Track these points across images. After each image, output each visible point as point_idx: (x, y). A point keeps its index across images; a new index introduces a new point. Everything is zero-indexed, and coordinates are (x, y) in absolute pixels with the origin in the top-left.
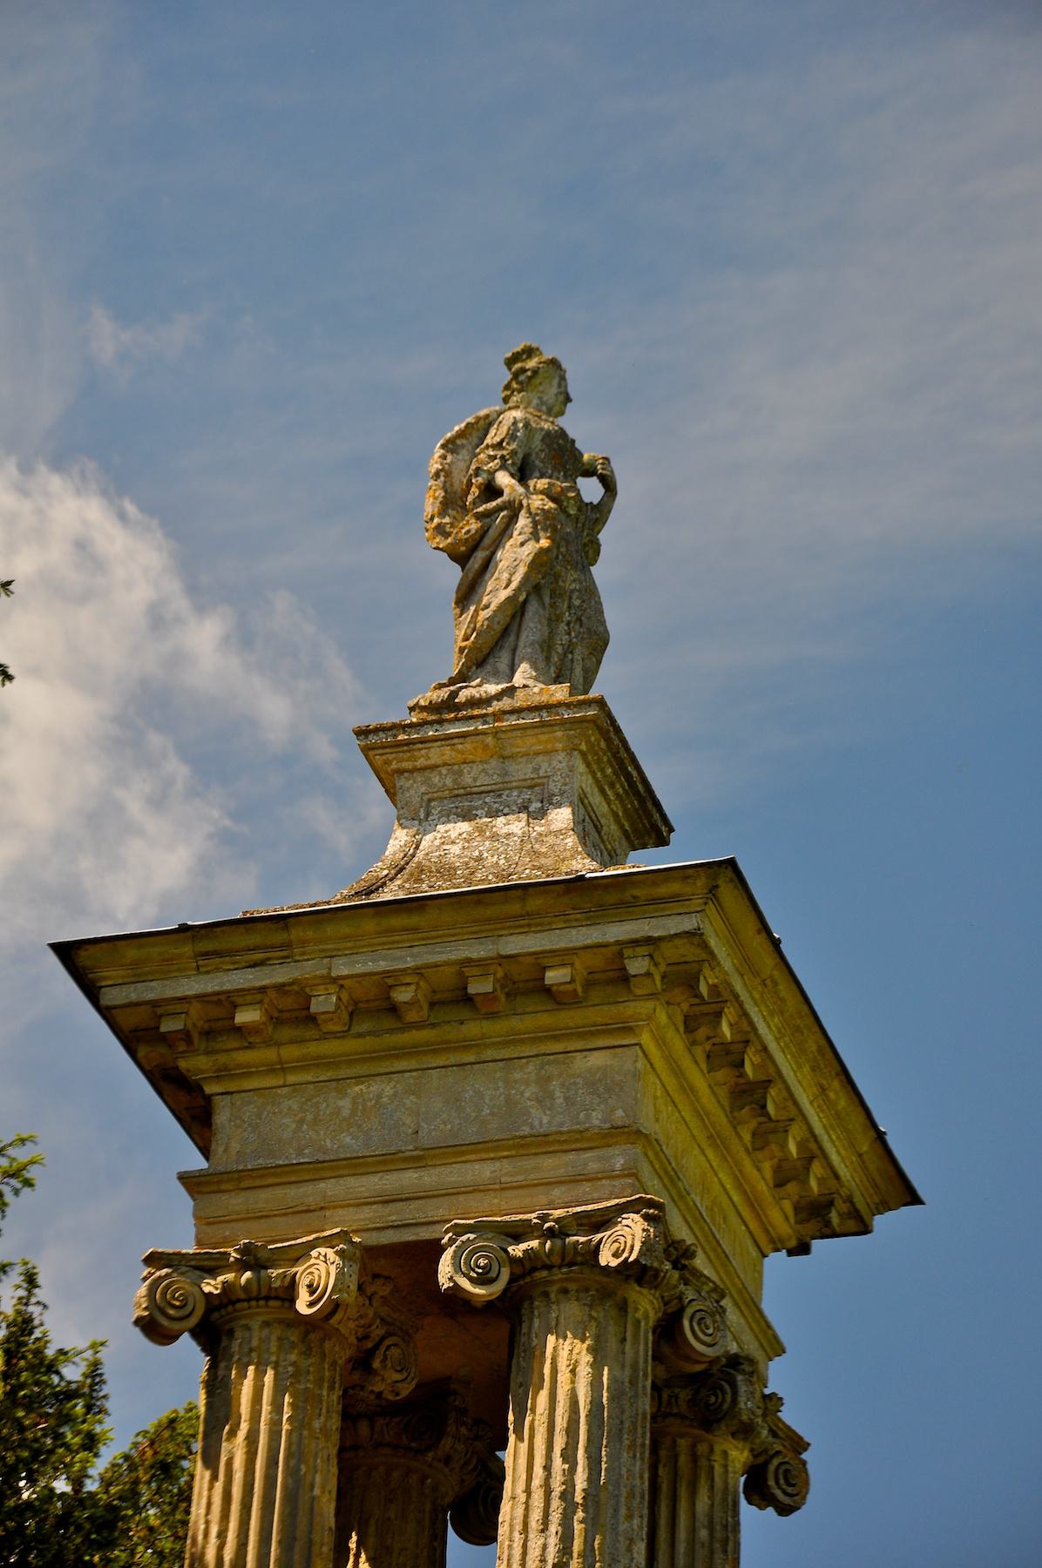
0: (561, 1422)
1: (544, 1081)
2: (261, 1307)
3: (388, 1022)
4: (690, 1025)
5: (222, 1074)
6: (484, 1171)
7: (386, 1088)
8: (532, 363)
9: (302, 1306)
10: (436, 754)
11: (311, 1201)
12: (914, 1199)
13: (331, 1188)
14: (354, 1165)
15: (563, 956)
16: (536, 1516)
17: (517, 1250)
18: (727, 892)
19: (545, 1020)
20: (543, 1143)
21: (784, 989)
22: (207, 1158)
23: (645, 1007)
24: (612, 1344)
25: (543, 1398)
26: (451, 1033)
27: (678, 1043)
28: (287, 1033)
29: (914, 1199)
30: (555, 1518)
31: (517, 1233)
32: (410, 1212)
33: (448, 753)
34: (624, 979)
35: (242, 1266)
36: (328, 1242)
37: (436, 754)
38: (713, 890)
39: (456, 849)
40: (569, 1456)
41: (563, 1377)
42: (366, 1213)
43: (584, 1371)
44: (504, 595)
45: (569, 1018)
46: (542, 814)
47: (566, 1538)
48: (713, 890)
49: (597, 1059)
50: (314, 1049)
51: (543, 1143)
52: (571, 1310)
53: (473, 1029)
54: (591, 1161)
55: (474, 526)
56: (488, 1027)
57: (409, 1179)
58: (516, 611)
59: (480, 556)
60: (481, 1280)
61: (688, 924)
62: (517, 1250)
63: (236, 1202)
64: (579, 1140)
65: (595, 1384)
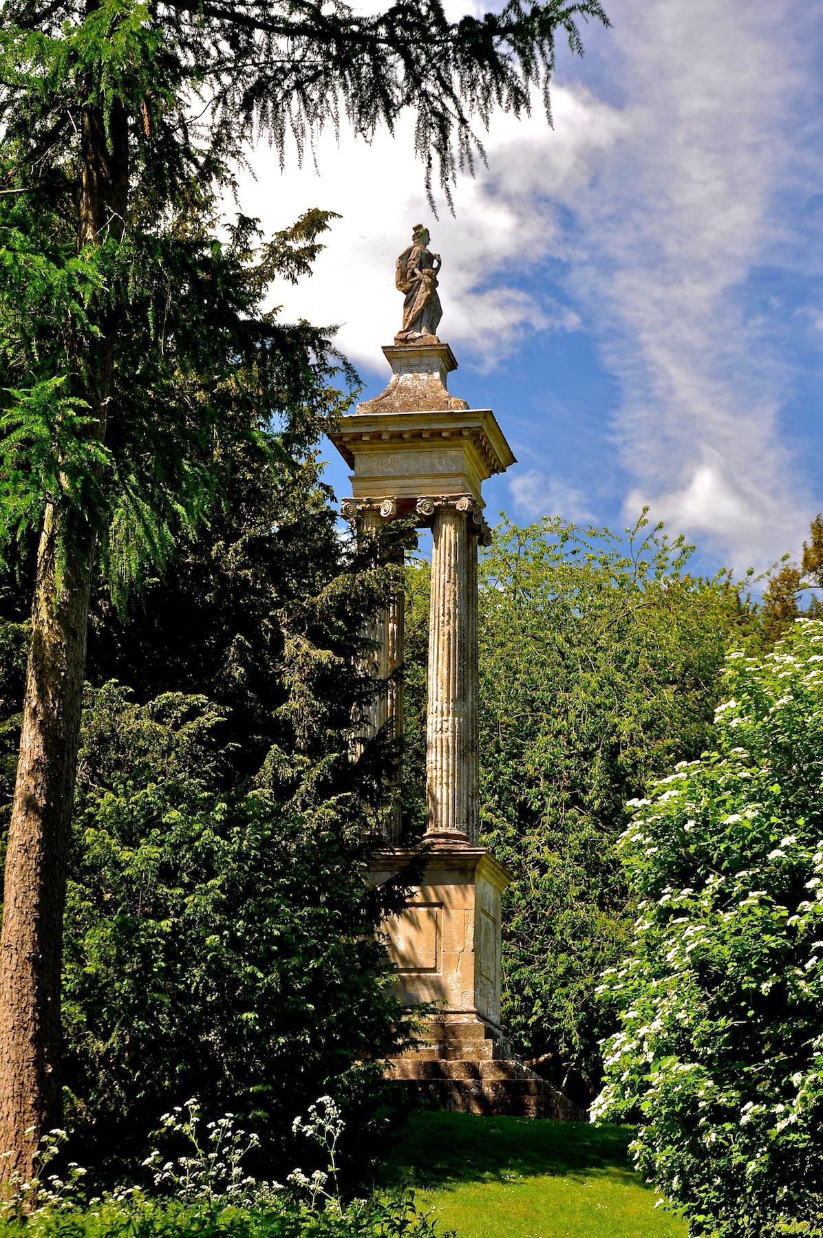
0: (447, 547)
1: (440, 458)
2: (140, 120)
3: (400, 441)
4: (475, 442)
5: (357, 450)
6: (426, 481)
7: (400, 457)
8: (421, 231)
9: (382, 513)
10: (403, 355)
11: (383, 486)
12: (516, 461)
13: (387, 482)
14: (394, 478)
15: (447, 430)
16: (442, 569)
17: (436, 504)
18: (489, 417)
19: (441, 443)
20: (441, 476)
21: (497, 431)
22: (353, 468)
23: (466, 442)
24: (458, 528)
25: (443, 539)
26: (416, 444)
27: (472, 447)
28: (375, 441)
29: (516, 461)
30: (447, 570)
31: (436, 499)
32: (407, 491)
33: (406, 354)
34: (461, 434)
35: (367, 503)
36: (389, 499)
37: (403, 355)
38: (485, 417)
39: (409, 383)
40: (449, 555)
41: (448, 535)
42: (397, 490)
43: (453, 534)
44: (419, 307)
45: (446, 443)
46: (431, 373)
47: (450, 575)
48: (485, 417)
49: (453, 453)
50: (381, 446)
51: (441, 476)
52: (449, 518)
53: (422, 444)
54: (453, 481)
55: (410, 285)
56: (426, 443)
57: (407, 482)
58: (422, 311)
59: (411, 293)
60: (428, 511)
61: (479, 424)
62: (436, 504)
63: (363, 484)
64: (450, 475)
65: (455, 538)
